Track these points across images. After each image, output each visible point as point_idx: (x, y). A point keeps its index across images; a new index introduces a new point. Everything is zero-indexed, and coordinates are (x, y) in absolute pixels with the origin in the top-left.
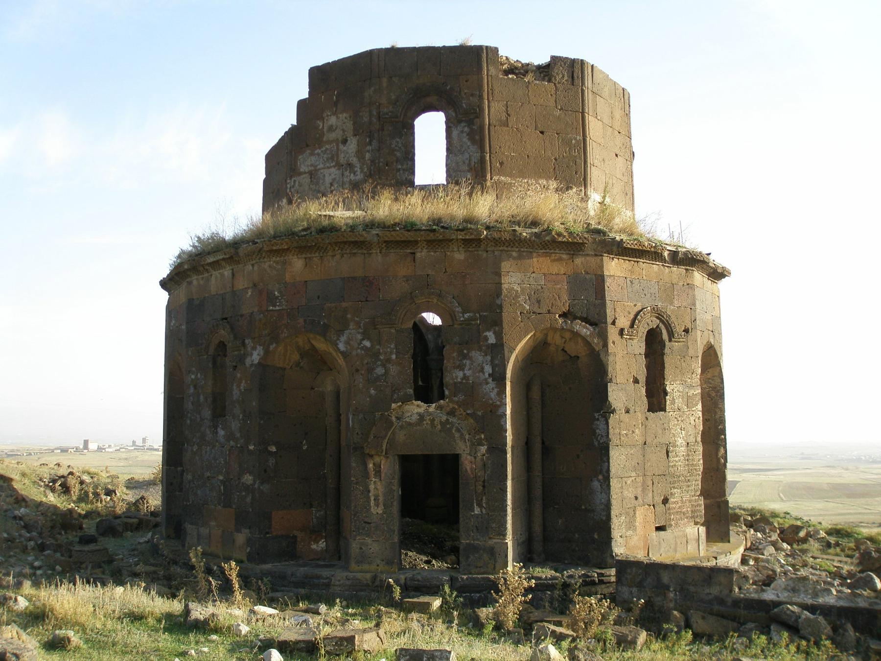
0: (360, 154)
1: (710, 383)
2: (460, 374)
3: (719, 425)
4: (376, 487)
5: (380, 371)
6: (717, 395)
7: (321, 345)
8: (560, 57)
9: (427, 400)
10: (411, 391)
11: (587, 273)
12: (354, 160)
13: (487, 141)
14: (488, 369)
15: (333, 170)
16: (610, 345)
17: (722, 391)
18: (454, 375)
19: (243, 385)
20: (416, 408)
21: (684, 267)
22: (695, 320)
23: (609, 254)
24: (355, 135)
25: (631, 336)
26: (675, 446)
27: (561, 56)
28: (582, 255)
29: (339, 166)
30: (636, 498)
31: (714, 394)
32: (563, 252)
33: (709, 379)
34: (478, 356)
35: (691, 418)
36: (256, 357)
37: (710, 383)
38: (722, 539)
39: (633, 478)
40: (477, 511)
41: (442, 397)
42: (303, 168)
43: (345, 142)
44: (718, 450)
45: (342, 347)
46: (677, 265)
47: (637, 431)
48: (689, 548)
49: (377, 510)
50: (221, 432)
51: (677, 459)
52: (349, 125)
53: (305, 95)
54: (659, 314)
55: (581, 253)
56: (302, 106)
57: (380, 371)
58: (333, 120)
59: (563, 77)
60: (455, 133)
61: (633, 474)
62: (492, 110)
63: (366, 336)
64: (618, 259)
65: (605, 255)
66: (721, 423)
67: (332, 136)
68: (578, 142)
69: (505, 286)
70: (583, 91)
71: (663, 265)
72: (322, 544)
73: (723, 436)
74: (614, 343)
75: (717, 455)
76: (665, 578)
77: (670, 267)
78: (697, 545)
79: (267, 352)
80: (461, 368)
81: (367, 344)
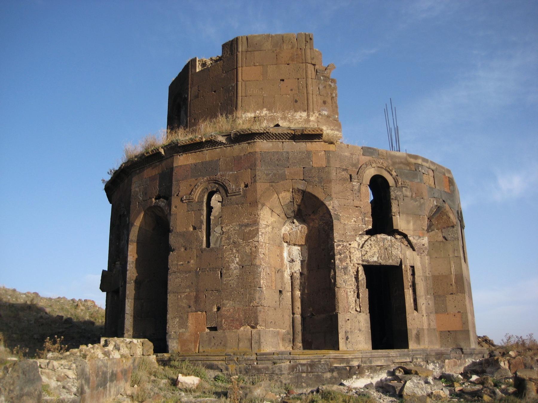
1: (324, 220)
3: (331, 252)
6: (328, 228)
8: (226, 43)
11: (167, 169)
13: (189, 110)
16: (173, 208)
17: (331, 224)
21: (245, 142)
22: (255, 176)
23: (177, 153)
25: (189, 200)
26: (228, 268)
27: (226, 42)
28: (164, 159)
30: (190, 307)
31: (326, 228)
32: (157, 161)
33: (322, 216)
35: (246, 248)
37: (324, 220)
38: (334, 347)
39: (187, 293)
44: (330, 272)
46: (238, 143)
47: (192, 261)
48: (240, 345)
51: (230, 278)
54: (215, 180)
55: (163, 159)
59: (227, 52)
61: (188, 290)
62: (192, 92)
64: (186, 154)
65: (174, 155)
66: (332, 250)
68: (233, 87)
69: (133, 190)
70: (237, 55)
71: (225, 147)
73: (332, 261)
74: (176, 207)
75: (329, 276)
77: (233, 146)
78: (249, 344)
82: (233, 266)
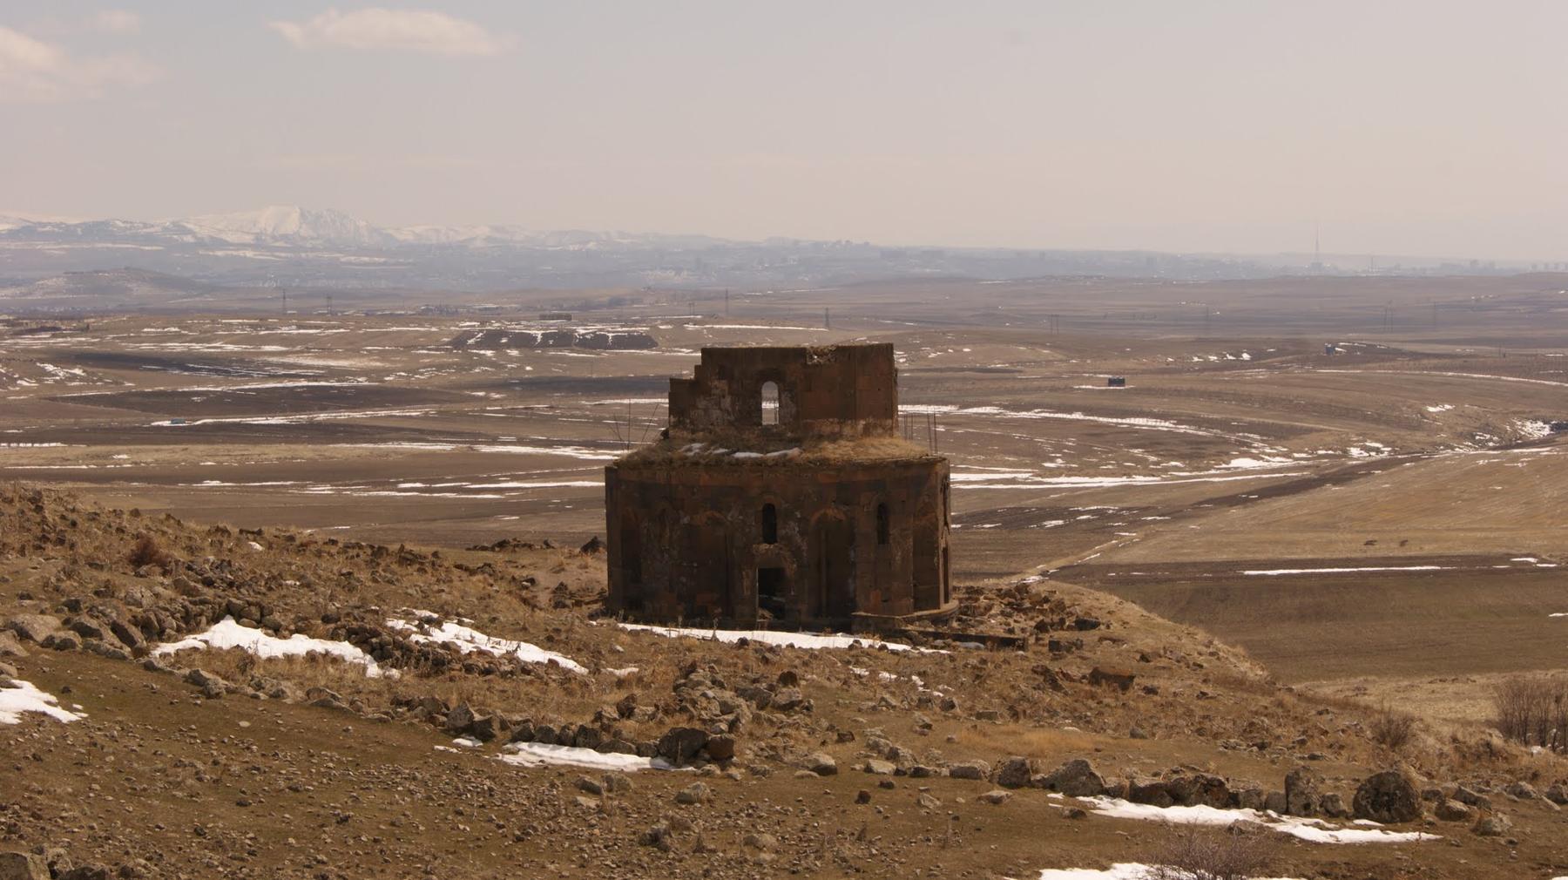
0: (733, 404)
2: (784, 532)
4: (746, 583)
5: (747, 530)
7: (717, 515)
9: (770, 543)
10: (761, 539)
12: (730, 409)
14: (797, 529)
15: (718, 411)
18: (781, 532)
19: (679, 533)
20: (765, 546)
24: (730, 393)
29: (721, 409)
34: (792, 524)
36: (686, 520)
40: (792, 593)
41: (776, 541)
42: (700, 407)
43: (724, 397)
45: (729, 518)
49: (747, 593)
50: (666, 556)
52: (726, 388)
53: (700, 363)
56: (697, 367)
57: (747, 530)
58: (716, 383)
60: (783, 396)
63: (741, 514)
67: (717, 392)
72: (720, 610)
76: (870, 622)
79: (692, 518)
80: (785, 528)
81: (741, 517)
82: (897, 558)
